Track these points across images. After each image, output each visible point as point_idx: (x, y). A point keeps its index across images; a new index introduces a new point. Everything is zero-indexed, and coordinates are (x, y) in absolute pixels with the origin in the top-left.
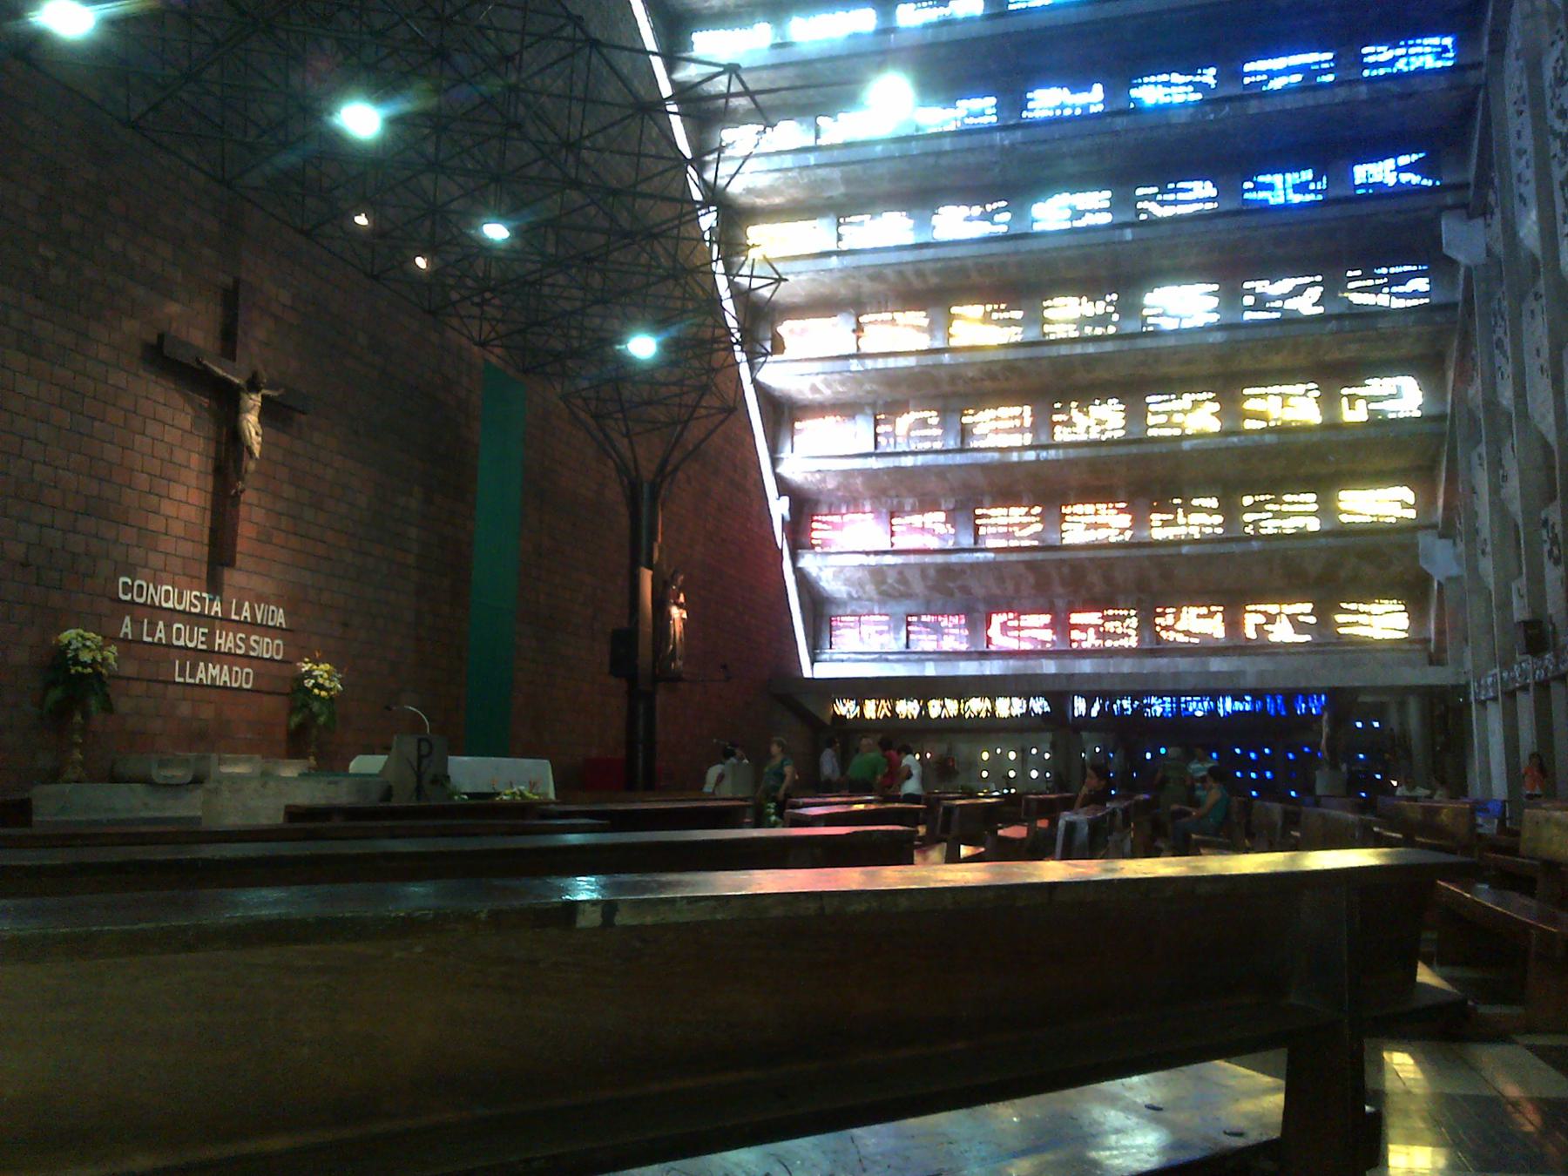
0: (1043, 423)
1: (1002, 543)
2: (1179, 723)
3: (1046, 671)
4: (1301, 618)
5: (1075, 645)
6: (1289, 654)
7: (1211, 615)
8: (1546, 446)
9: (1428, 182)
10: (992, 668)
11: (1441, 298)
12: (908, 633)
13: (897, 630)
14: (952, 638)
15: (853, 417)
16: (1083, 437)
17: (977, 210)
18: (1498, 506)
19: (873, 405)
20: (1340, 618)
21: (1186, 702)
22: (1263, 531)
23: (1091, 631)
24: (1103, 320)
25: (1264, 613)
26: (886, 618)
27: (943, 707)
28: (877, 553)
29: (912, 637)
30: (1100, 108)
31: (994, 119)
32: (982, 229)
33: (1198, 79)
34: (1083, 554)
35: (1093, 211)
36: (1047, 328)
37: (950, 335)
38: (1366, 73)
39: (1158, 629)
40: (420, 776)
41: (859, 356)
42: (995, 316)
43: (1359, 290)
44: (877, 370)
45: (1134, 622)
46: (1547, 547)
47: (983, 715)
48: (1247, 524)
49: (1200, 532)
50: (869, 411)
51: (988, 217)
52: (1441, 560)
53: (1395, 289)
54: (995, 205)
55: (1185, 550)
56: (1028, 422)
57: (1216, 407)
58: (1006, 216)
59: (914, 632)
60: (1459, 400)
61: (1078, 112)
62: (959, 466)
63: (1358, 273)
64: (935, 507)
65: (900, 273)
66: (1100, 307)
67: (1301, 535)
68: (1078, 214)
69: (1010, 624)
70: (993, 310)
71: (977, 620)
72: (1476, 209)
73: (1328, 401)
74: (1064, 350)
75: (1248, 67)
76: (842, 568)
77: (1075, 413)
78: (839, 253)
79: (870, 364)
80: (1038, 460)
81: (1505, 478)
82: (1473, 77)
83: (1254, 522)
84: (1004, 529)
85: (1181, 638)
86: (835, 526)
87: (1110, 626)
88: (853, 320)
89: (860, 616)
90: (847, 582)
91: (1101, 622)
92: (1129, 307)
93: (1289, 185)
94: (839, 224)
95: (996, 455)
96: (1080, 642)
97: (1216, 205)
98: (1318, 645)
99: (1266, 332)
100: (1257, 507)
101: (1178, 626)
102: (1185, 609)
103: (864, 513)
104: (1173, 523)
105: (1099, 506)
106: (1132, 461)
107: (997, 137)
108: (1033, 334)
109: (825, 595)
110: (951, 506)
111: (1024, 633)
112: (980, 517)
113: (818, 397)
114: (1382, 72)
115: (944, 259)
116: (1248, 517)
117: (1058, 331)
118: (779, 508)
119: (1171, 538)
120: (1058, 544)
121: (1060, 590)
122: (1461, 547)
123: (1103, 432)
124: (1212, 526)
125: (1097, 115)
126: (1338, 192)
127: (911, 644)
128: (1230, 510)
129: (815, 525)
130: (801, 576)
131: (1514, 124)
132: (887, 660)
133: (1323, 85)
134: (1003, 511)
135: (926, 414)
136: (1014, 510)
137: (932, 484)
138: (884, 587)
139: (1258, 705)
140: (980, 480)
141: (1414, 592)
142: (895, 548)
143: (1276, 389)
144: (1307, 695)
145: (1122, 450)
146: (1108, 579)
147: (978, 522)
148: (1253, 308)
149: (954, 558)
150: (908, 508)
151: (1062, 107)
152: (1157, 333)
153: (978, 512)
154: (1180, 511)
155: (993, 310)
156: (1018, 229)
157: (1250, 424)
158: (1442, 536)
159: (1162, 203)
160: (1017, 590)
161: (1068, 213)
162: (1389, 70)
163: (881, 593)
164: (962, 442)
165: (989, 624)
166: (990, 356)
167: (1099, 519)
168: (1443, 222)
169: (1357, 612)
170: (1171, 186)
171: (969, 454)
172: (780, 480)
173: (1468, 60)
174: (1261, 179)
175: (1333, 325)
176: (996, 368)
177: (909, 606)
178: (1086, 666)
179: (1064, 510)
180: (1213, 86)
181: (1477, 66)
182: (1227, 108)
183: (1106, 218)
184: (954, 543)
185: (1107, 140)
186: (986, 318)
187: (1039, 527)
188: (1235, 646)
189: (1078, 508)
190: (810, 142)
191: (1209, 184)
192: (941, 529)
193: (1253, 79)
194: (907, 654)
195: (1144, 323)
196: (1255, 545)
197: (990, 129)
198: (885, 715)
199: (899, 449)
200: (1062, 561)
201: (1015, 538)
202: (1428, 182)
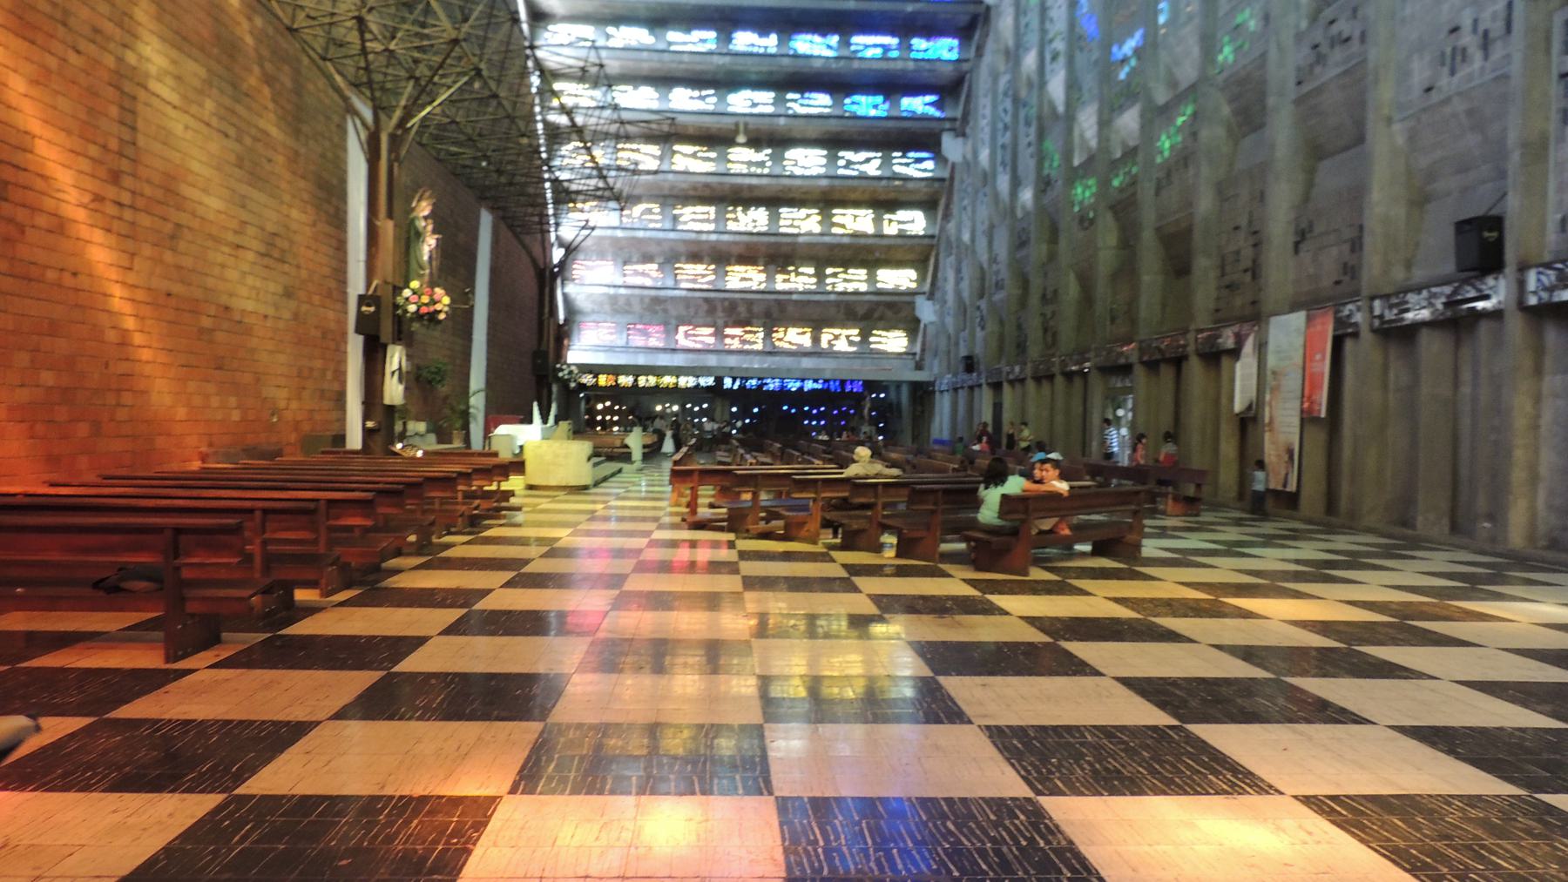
2: (783, 394)
6: (843, 357)
7: (804, 333)
8: (982, 268)
9: (937, 114)
10: (678, 360)
12: (629, 335)
13: (621, 332)
16: (742, 228)
17: (696, 93)
18: (958, 293)
20: (872, 339)
22: (836, 290)
24: (761, 164)
27: (647, 380)
28: (615, 286)
30: (773, 50)
32: (699, 106)
36: (729, 165)
38: (913, 55)
43: (901, 164)
45: (761, 335)
46: (978, 320)
47: (671, 386)
51: (702, 98)
52: (926, 312)
55: (794, 297)
56: (713, 216)
57: (819, 218)
58: (714, 100)
60: (942, 229)
61: (762, 51)
63: (900, 154)
67: (856, 293)
68: (754, 105)
71: (671, 330)
72: (961, 133)
73: (878, 221)
74: (739, 180)
76: (592, 295)
80: (717, 241)
81: (962, 279)
82: (965, 66)
83: (834, 284)
84: (693, 277)
85: (787, 346)
86: (588, 268)
87: (748, 337)
90: (594, 302)
92: (777, 158)
95: (693, 236)
99: (850, 182)
100: (835, 275)
105: (749, 268)
106: (770, 245)
108: (721, 169)
112: (677, 269)
114: (920, 56)
116: (829, 281)
117: (735, 168)
121: (720, 314)
122: (938, 307)
126: (894, 113)
128: (820, 276)
129: (574, 266)
130: (565, 296)
132: (615, 352)
137: (653, 249)
138: (615, 307)
139: (826, 386)
141: (912, 326)
143: (850, 211)
144: (852, 382)
146: (749, 310)
147: (677, 272)
148: (846, 167)
150: (635, 260)
151: (753, 45)
152: (792, 176)
153: (677, 265)
154: (793, 274)
156: (721, 109)
157: (835, 230)
158: (929, 299)
159: (802, 105)
160: (696, 313)
161: (750, 103)
164: (674, 225)
165: (676, 331)
167: (746, 276)
169: (880, 336)
172: (558, 237)
173: (963, 57)
174: (856, 98)
175: (884, 183)
177: (629, 318)
178: (732, 361)
181: (966, 61)
183: (770, 109)
186: (694, 155)
187: (713, 277)
188: (816, 353)
189: (737, 268)
192: (655, 274)
196: (832, 297)
197: (710, 53)
200: (725, 299)
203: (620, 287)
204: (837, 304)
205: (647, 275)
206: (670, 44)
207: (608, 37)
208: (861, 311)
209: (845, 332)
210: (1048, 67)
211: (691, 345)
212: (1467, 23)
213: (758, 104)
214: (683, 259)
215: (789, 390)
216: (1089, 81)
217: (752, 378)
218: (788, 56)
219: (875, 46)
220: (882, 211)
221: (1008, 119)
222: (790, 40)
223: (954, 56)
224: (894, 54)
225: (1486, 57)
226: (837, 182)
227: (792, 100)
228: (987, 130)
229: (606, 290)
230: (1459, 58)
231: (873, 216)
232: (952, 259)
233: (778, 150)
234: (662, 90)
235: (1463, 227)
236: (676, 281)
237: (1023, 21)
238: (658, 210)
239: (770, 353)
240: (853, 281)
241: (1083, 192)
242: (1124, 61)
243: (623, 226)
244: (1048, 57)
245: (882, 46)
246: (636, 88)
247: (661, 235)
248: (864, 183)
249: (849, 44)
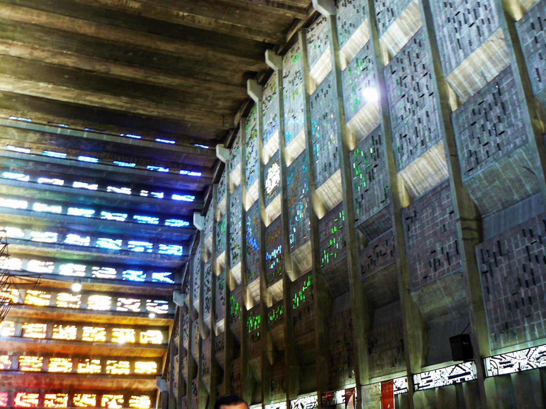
1: (28, 369)
4: (119, 401)
7: (92, 397)
8: (195, 362)
9: (171, 281)
11: (171, 312)
17: (44, 263)
24: (76, 303)
38: (160, 252)
42: (42, 296)
45: (66, 398)
46: (193, 390)
53: (160, 307)
56: (45, 330)
57: (105, 333)
58: (53, 267)
60: (172, 340)
63: (150, 301)
68: (74, 272)
75: (130, 242)
81: (183, 368)
87: (59, 400)
100: (112, 364)
102: (84, 395)
104: (85, 367)
108: (52, 304)
110: (12, 354)
117: (60, 304)
126: (149, 280)
128: (103, 365)
131: (195, 276)
134: (29, 357)
153: (21, 357)
154: (88, 363)
157: (113, 340)
158: (162, 378)
161: (72, 270)
167: (62, 364)
168: (174, 293)
173: (185, 254)
174: (129, 271)
181: (188, 256)
187: (41, 365)
189: (56, 359)
191: (114, 270)
202: (171, 281)
209: (116, 397)
210: (232, 261)
212: (438, 249)
216: (254, 268)
218: (94, 247)
219: (141, 246)
220: (140, 330)
221: (210, 286)
223: (180, 254)
224: (150, 251)
225: (449, 265)
227: (95, 270)
228: (198, 291)
230: (437, 264)
232: (177, 357)
234: (24, 260)
235: (453, 340)
237: (217, 239)
240: (123, 368)
241: (254, 323)
242: (273, 259)
244: (231, 257)
245: (144, 247)
249: (127, 245)
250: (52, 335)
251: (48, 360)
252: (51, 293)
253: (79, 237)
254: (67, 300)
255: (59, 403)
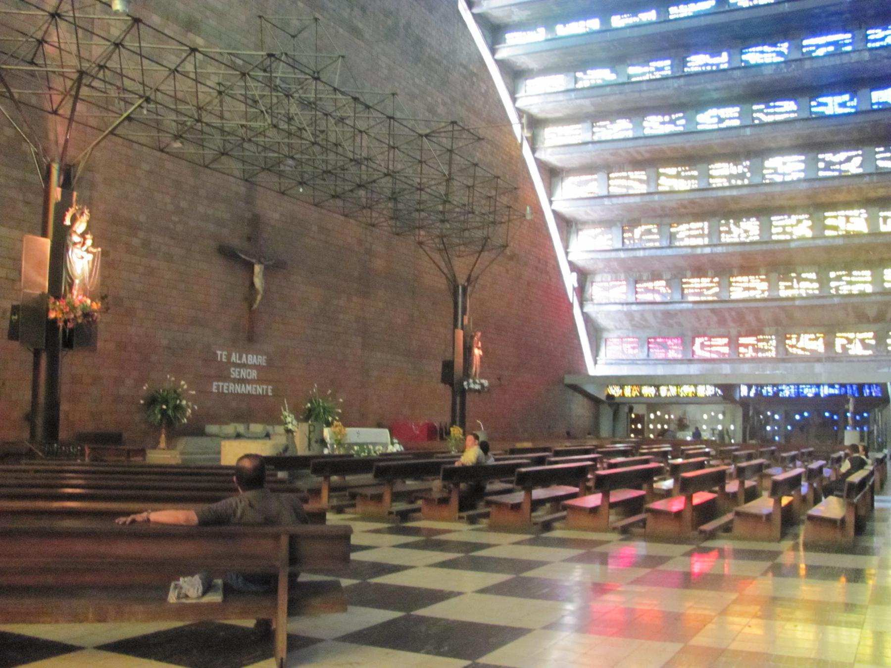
0: (715, 232)
1: (697, 299)
3: (724, 372)
4: (867, 341)
5: (741, 356)
6: (859, 361)
7: (817, 339)
10: (694, 369)
12: (649, 348)
13: (642, 346)
14: (673, 351)
15: (610, 227)
16: (736, 240)
17: (667, 118)
19: (621, 222)
21: (803, 389)
22: (841, 292)
23: (750, 348)
24: (742, 176)
25: (847, 338)
26: (635, 340)
27: (668, 390)
28: (627, 304)
29: (651, 350)
30: (725, 66)
31: (669, 73)
32: (669, 129)
33: (777, 49)
34: (741, 305)
35: (730, 119)
36: (711, 181)
37: (658, 185)
39: (787, 346)
40: (310, 440)
41: (609, 196)
42: (683, 174)
43: (883, 159)
44: (618, 204)
45: (774, 343)
47: (690, 395)
48: (831, 288)
49: (807, 293)
50: (619, 225)
51: (673, 122)
54: (677, 115)
55: (797, 303)
56: (706, 232)
57: (810, 223)
58: (683, 122)
59: (652, 348)
61: (714, 68)
62: (669, 256)
63: (882, 149)
64: (660, 278)
65: (628, 153)
66: (740, 169)
67: (862, 294)
68: (721, 120)
69: (706, 343)
70: (682, 171)
71: (687, 342)
74: (720, 193)
75: (805, 42)
77: (732, 226)
78: (593, 143)
79: (615, 200)
80: (712, 253)
83: (837, 288)
84: (699, 290)
85: (800, 352)
87: (761, 345)
88: (606, 176)
89: (622, 338)
91: (756, 342)
92: (757, 170)
93: (836, 103)
94: (593, 127)
95: (689, 250)
96: (744, 354)
97: (796, 115)
98: (876, 356)
99: (830, 183)
100: (838, 278)
101: (800, 345)
103: (620, 281)
104: (791, 287)
105: (751, 277)
106: (765, 253)
107: (671, 81)
108: (703, 185)
109: (602, 326)
110: (669, 277)
111: (714, 349)
112: (685, 283)
113: (590, 218)
115: (649, 145)
116: (833, 284)
117: (716, 183)
118: (570, 280)
119: (790, 296)
120: (727, 299)
121: (732, 324)
123: (747, 237)
124: (813, 289)
125: (724, 70)
127: (650, 355)
128: (823, 281)
132: (637, 364)
133: (847, 53)
135: (651, 227)
136: (704, 280)
138: (633, 323)
140: (682, 263)
142: (638, 301)
143: (842, 213)
144: (870, 386)
145: (758, 248)
146: (758, 319)
147: (684, 286)
148: (824, 169)
149: (670, 307)
150: (645, 278)
151: (706, 65)
152: (773, 184)
153: (684, 280)
155: (682, 171)
156: (691, 128)
157: (828, 233)
159: (767, 114)
160: (709, 324)
161: (716, 120)
162: (882, 43)
163: (633, 326)
164: (670, 243)
165: (693, 343)
166: (681, 196)
167: (751, 285)
170: (772, 104)
171: (674, 249)
172: (571, 264)
174: (821, 100)
175: (867, 179)
176: (686, 202)
178: (746, 368)
179: (732, 279)
180: (786, 53)
182: (793, 66)
183: (737, 123)
184: (671, 299)
185: (730, 82)
186: (678, 176)
187: (717, 289)
189: (739, 279)
190: (571, 86)
192: (663, 290)
193: (808, 49)
194: (647, 361)
195: (766, 179)
196: (836, 300)
197: (665, 78)
198: (636, 395)
199: (636, 247)
200: (731, 309)
201: (704, 295)
203: (632, 304)
204: (844, 307)
205: (658, 292)
206: (629, 77)
207: (576, 80)
208: (872, 313)
211: (707, 355)
213: (726, 119)
214: (689, 273)
215: (806, 396)
217: (767, 386)
218: (739, 68)
220: (877, 209)
222: (742, 53)
226: (817, 185)
229: (619, 307)
231: (866, 216)
233: (757, 161)
236: (683, 294)
238: (655, 231)
239: (783, 360)
243: (626, 247)
245: (834, 43)
246: (612, 122)
247: (659, 253)
248: (845, 181)
250: (720, 237)
251: (726, 281)
252: (699, 166)
253: (708, 56)
254: (727, 173)
255: (764, 351)
